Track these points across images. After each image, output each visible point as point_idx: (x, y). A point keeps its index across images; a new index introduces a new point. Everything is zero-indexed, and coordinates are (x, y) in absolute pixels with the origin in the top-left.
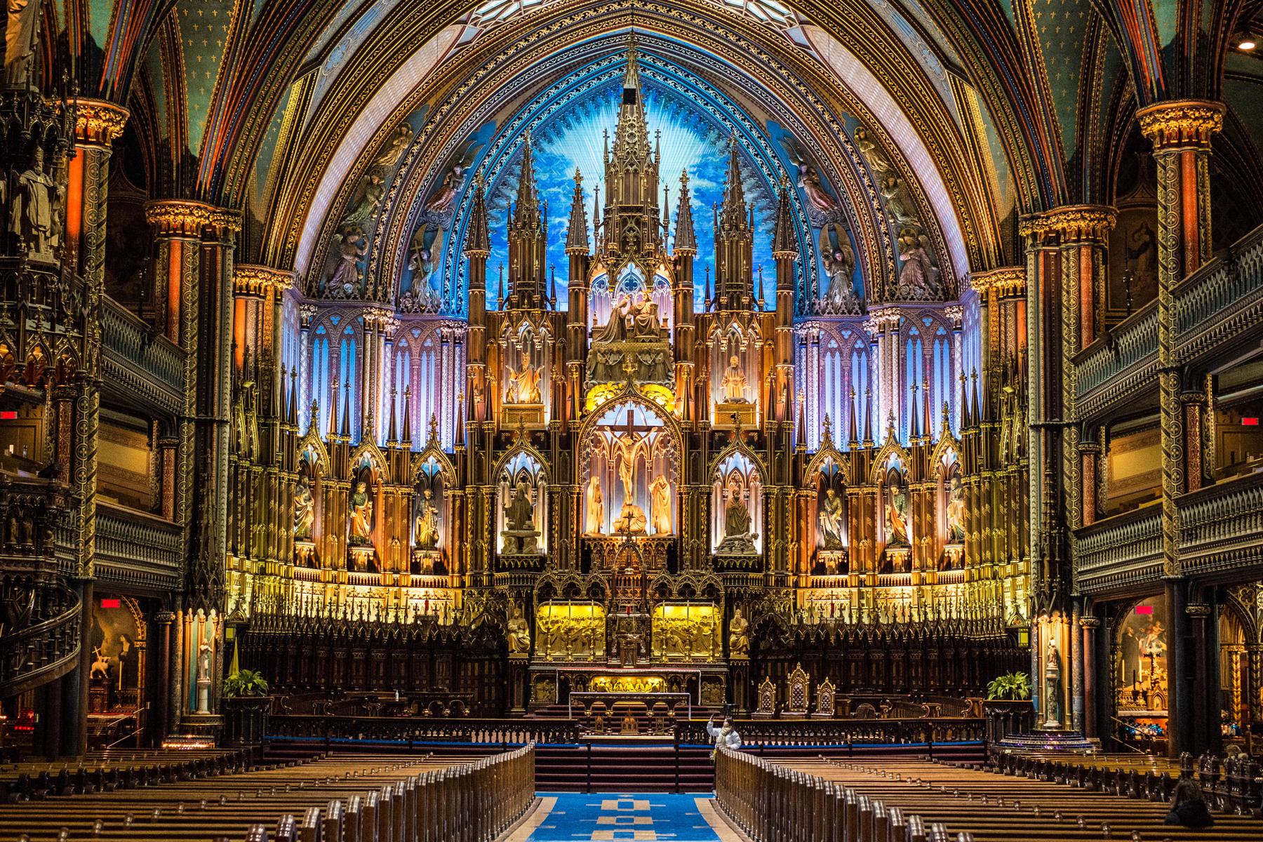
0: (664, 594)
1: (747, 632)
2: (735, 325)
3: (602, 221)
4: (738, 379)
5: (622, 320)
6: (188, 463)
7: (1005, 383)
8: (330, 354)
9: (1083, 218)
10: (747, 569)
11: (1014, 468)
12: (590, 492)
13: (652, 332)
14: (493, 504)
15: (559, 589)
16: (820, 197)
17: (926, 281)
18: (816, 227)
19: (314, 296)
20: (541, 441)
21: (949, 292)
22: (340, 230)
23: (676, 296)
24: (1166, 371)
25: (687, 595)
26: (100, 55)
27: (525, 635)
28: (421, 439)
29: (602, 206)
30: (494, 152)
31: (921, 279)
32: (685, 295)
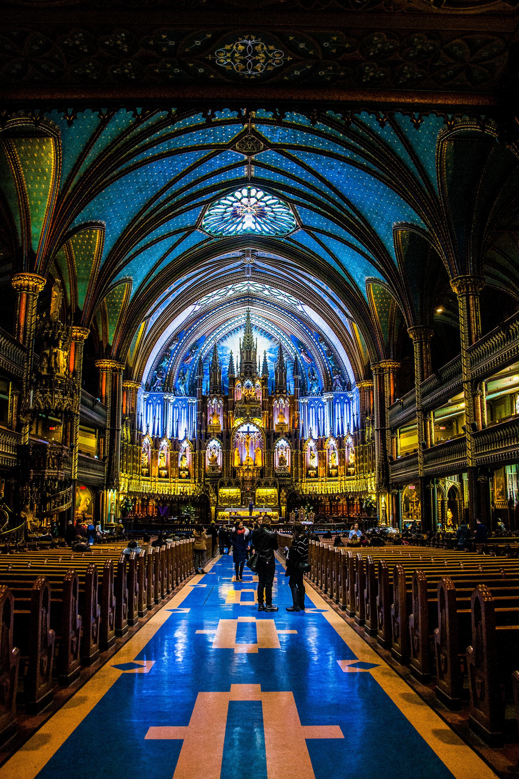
0: (259, 485)
1: (286, 496)
2: (282, 400)
3: (239, 366)
5: (245, 398)
6: (108, 443)
7: (367, 416)
9: (391, 364)
10: (286, 477)
11: (369, 443)
12: (236, 453)
13: (255, 401)
14: (205, 456)
15: (226, 483)
19: (148, 391)
20: (220, 437)
21: (348, 387)
23: (262, 390)
24: (418, 411)
25: (267, 485)
26: (81, 312)
27: (215, 498)
28: (181, 437)
29: (239, 362)
30: (205, 345)
32: (265, 390)
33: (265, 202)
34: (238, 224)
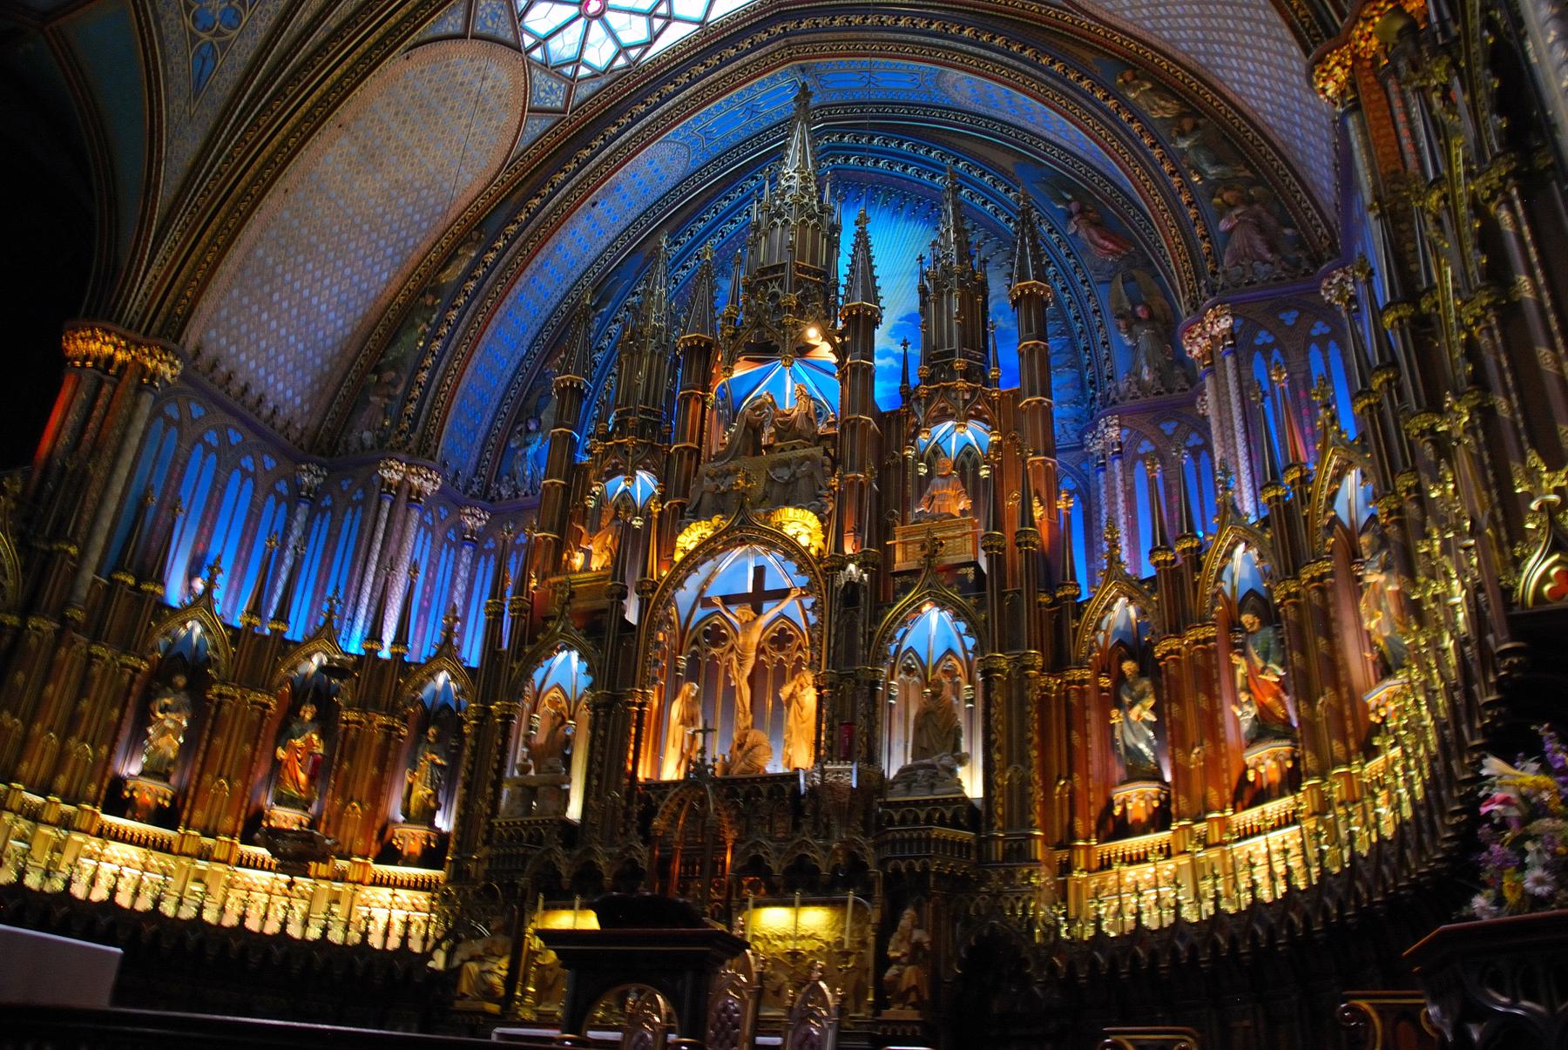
4: (950, 492)
8: (330, 530)
13: (799, 437)
14: (506, 736)
16: (1104, 238)
17: (1272, 248)
18: (1102, 282)
19: (322, 454)
22: (377, 370)
31: (1261, 248)
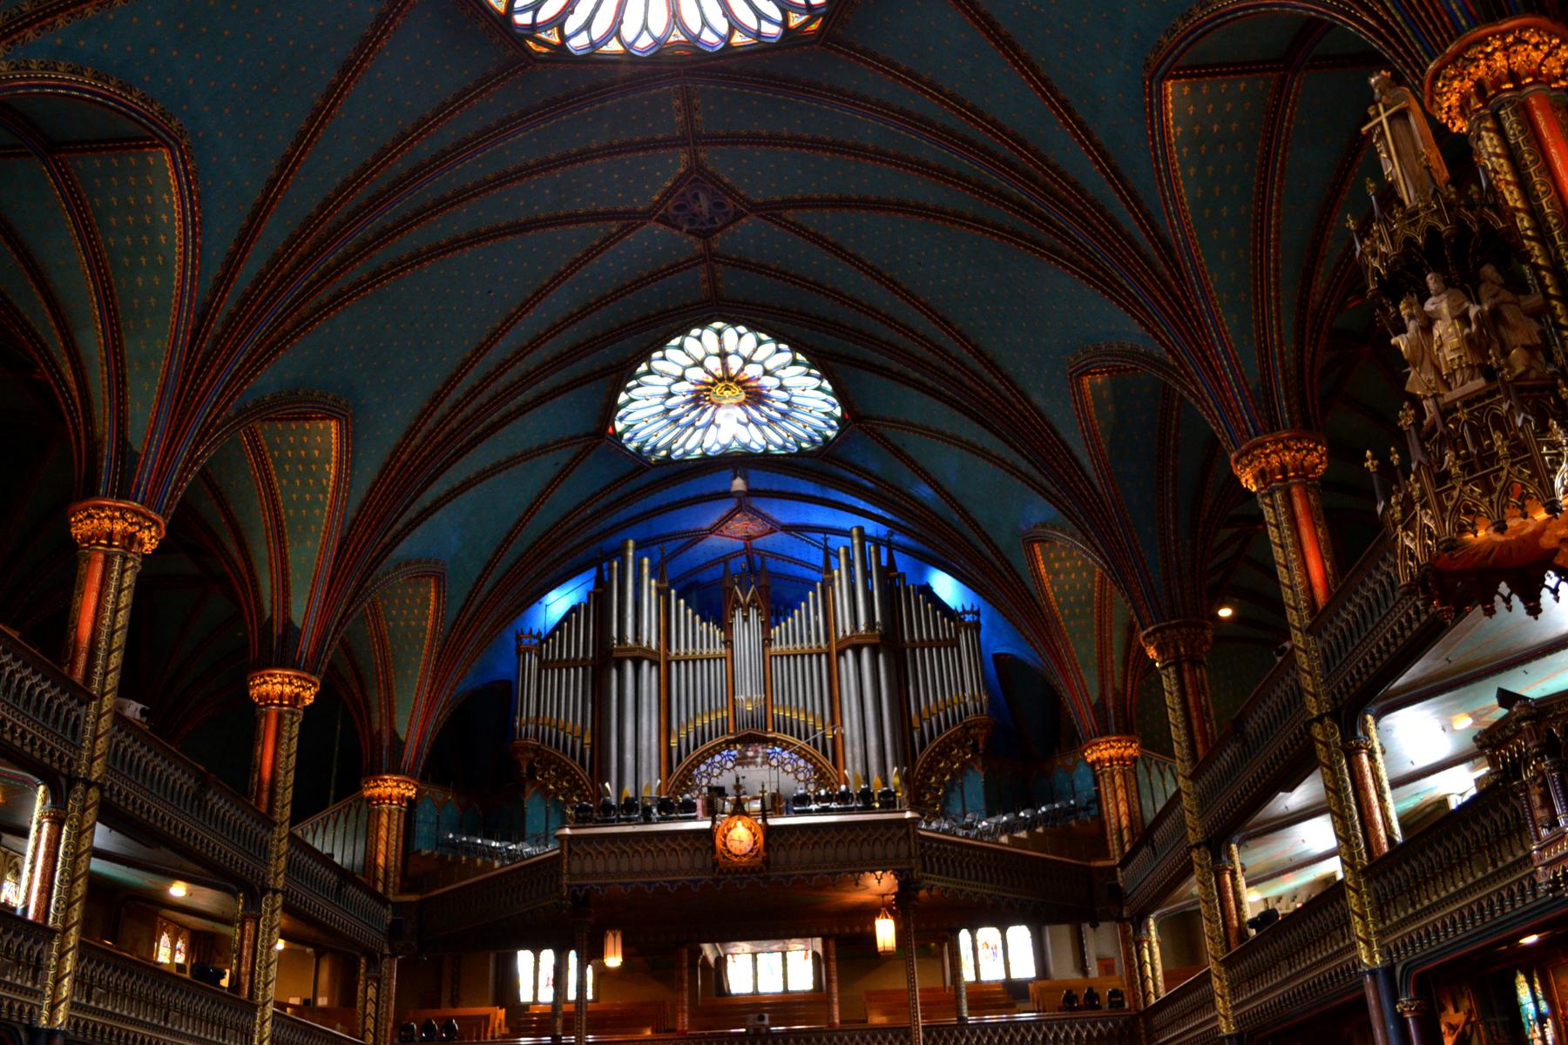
33: (762, 363)
34: (707, 426)
